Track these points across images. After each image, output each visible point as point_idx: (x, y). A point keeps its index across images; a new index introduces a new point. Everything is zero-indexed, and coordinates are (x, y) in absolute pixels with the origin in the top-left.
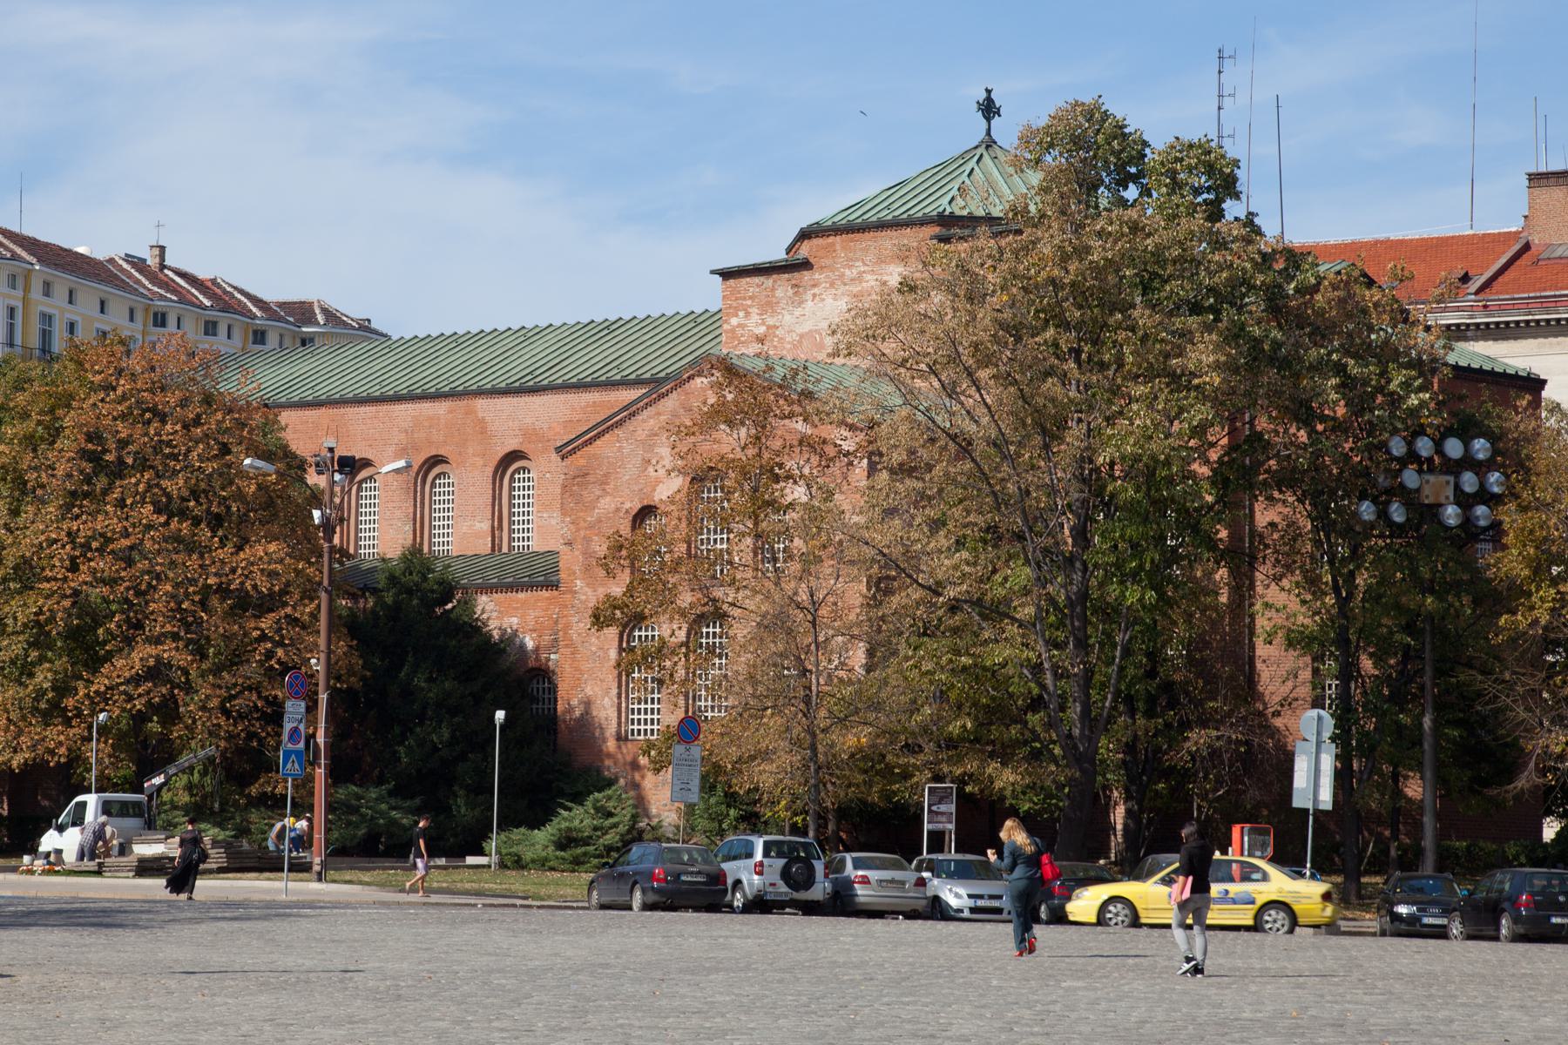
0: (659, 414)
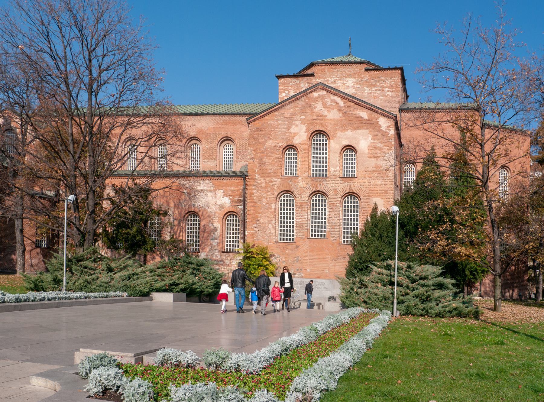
0: (295, 107)
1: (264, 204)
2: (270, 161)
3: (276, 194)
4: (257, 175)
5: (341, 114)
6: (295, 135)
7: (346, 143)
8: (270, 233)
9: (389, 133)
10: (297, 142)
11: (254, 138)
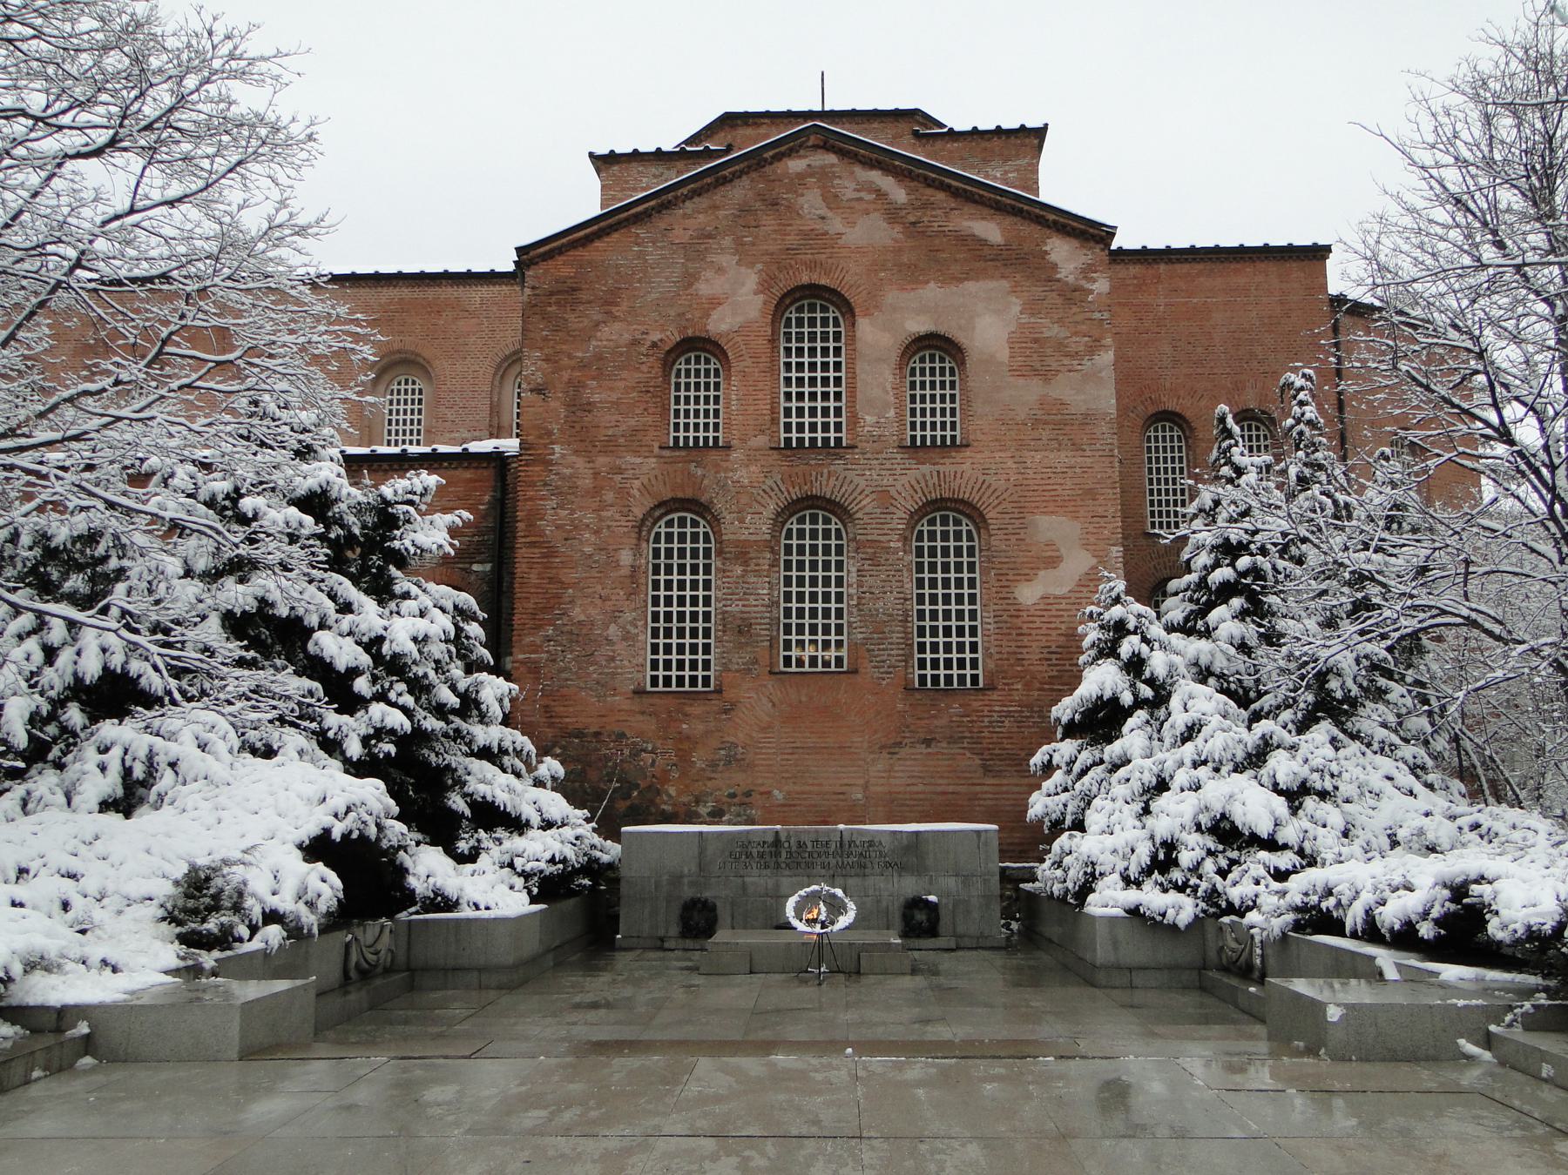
0: (716, 207)
1: (588, 550)
2: (614, 397)
3: (639, 512)
4: (557, 448)
5: (898, 228)
6: (715, 302)
7: (919, 325)
8: (613, 659)
9: (1091, 292)
10: (724, 327)
11: (545, 317)
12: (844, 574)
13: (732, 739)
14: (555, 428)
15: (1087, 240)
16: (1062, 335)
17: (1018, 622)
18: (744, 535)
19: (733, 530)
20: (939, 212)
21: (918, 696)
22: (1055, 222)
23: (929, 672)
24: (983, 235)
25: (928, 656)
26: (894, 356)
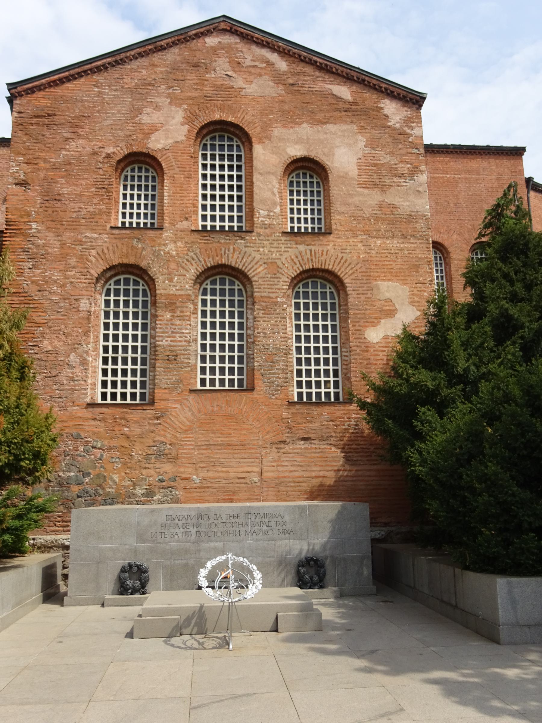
0: (154, 65)
2: (78, 190)
3: (95, 273)
4: (34, 225)
5: (281, 87)
6: (153, 129)
9: (411, 135)
10: (160, 146)
12: (244, 321)
13: (162, 439)
14: (33, 210)
15: (407, 101)
16: (392, 162)
17: (367, 355)
18: (173, 291)
19: (164, 287)
20: (308, 78)
21: (298, 407)
22: (386, 89)
23: (304, 390)
24: (339, 95)
25: (304, 379)
26: (280, 170)
